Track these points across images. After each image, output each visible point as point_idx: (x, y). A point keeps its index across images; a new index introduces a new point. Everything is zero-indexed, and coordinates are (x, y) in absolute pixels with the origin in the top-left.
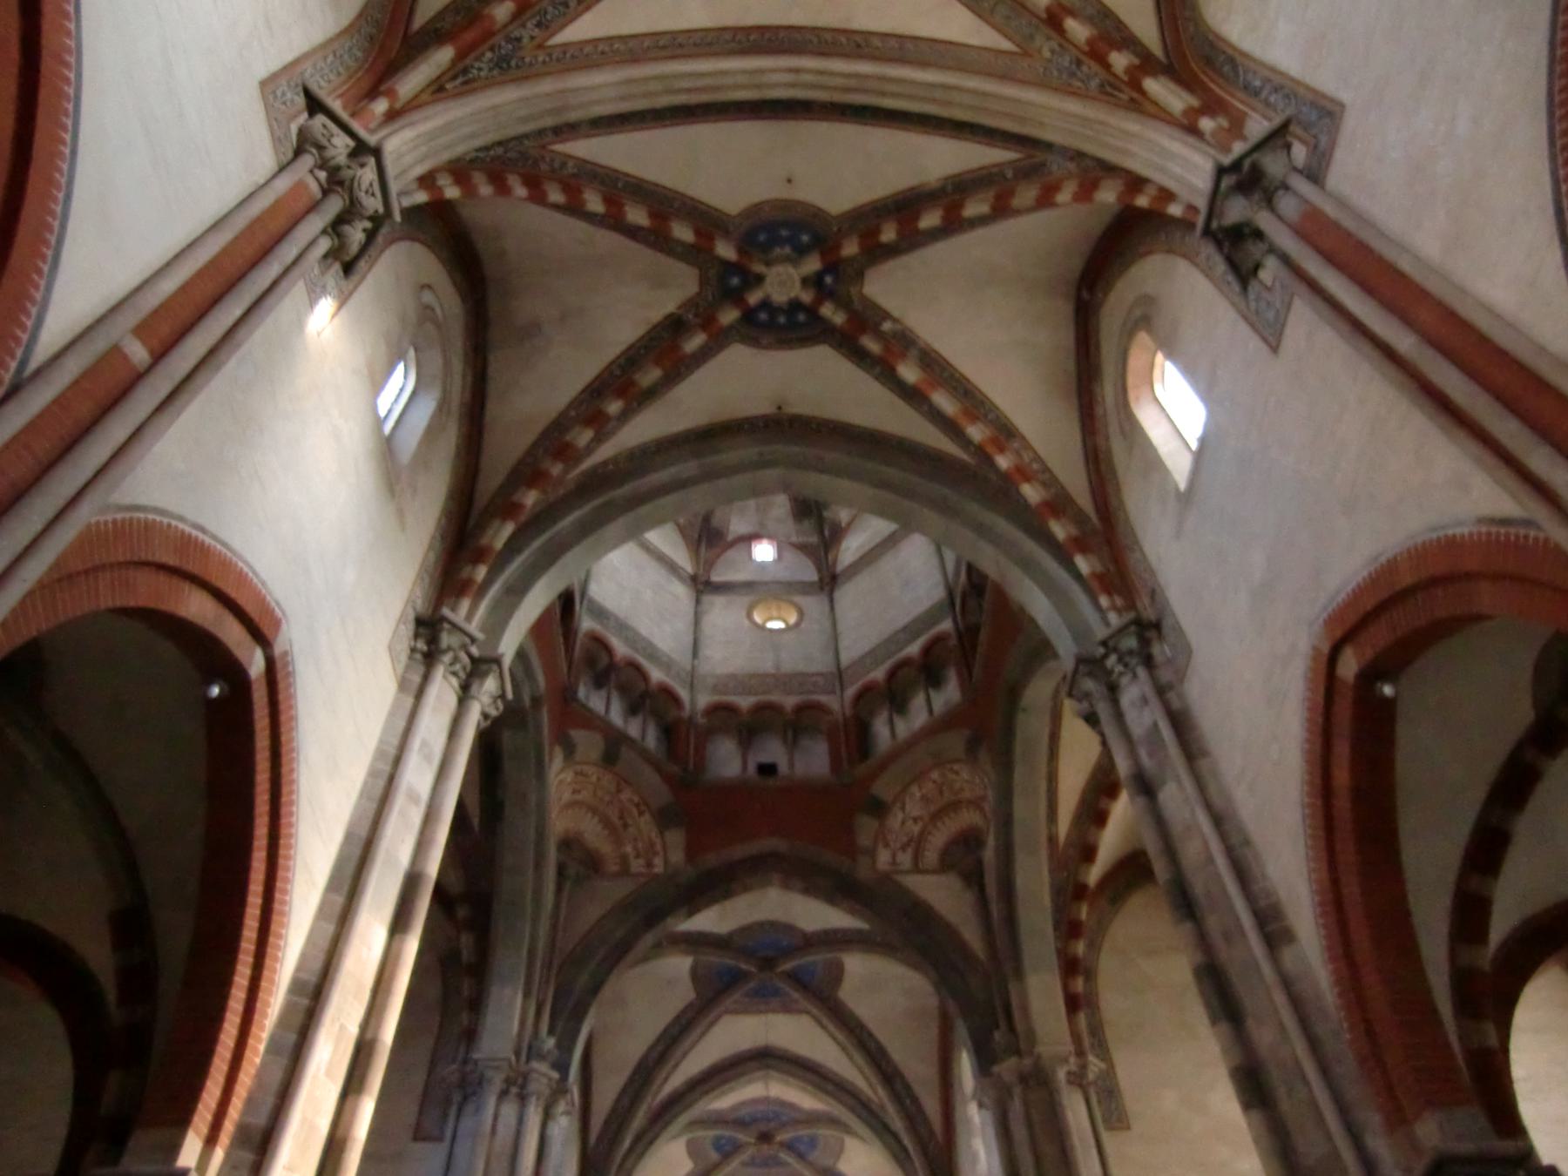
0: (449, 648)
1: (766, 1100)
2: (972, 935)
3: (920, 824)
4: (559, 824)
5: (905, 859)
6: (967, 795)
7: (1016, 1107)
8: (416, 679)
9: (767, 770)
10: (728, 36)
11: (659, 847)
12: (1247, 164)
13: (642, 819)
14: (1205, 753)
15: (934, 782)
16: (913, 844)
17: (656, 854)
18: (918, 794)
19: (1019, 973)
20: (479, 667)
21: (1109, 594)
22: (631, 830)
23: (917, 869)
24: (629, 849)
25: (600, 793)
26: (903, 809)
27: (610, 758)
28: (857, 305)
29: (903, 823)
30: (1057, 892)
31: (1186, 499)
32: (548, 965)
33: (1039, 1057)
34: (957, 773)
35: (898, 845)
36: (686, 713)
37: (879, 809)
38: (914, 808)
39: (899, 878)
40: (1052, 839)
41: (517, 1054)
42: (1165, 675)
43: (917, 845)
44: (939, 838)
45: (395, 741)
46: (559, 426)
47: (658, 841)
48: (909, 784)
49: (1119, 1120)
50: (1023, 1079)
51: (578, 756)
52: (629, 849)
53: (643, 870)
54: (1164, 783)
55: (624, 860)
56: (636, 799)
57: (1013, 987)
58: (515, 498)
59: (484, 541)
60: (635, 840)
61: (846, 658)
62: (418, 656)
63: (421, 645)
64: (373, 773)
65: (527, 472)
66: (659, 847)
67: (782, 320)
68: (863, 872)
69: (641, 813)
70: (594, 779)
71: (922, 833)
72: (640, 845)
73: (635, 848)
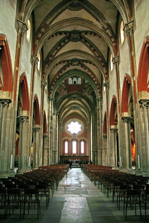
5: (87, 94)
8: (49, 102)
9: (75, 82)
23: (88, 95)
24: (61, 92)
28: (82, 64)
31: (104, 93)
32: (55, 104)
39: (87, 96)
42: (102, 102)
44: (91, 92)
46: (56, 76)
52: (61, 92)
55: (61, 93)
59: (51, 88)
65: (53, 81)
68: (83, 95)
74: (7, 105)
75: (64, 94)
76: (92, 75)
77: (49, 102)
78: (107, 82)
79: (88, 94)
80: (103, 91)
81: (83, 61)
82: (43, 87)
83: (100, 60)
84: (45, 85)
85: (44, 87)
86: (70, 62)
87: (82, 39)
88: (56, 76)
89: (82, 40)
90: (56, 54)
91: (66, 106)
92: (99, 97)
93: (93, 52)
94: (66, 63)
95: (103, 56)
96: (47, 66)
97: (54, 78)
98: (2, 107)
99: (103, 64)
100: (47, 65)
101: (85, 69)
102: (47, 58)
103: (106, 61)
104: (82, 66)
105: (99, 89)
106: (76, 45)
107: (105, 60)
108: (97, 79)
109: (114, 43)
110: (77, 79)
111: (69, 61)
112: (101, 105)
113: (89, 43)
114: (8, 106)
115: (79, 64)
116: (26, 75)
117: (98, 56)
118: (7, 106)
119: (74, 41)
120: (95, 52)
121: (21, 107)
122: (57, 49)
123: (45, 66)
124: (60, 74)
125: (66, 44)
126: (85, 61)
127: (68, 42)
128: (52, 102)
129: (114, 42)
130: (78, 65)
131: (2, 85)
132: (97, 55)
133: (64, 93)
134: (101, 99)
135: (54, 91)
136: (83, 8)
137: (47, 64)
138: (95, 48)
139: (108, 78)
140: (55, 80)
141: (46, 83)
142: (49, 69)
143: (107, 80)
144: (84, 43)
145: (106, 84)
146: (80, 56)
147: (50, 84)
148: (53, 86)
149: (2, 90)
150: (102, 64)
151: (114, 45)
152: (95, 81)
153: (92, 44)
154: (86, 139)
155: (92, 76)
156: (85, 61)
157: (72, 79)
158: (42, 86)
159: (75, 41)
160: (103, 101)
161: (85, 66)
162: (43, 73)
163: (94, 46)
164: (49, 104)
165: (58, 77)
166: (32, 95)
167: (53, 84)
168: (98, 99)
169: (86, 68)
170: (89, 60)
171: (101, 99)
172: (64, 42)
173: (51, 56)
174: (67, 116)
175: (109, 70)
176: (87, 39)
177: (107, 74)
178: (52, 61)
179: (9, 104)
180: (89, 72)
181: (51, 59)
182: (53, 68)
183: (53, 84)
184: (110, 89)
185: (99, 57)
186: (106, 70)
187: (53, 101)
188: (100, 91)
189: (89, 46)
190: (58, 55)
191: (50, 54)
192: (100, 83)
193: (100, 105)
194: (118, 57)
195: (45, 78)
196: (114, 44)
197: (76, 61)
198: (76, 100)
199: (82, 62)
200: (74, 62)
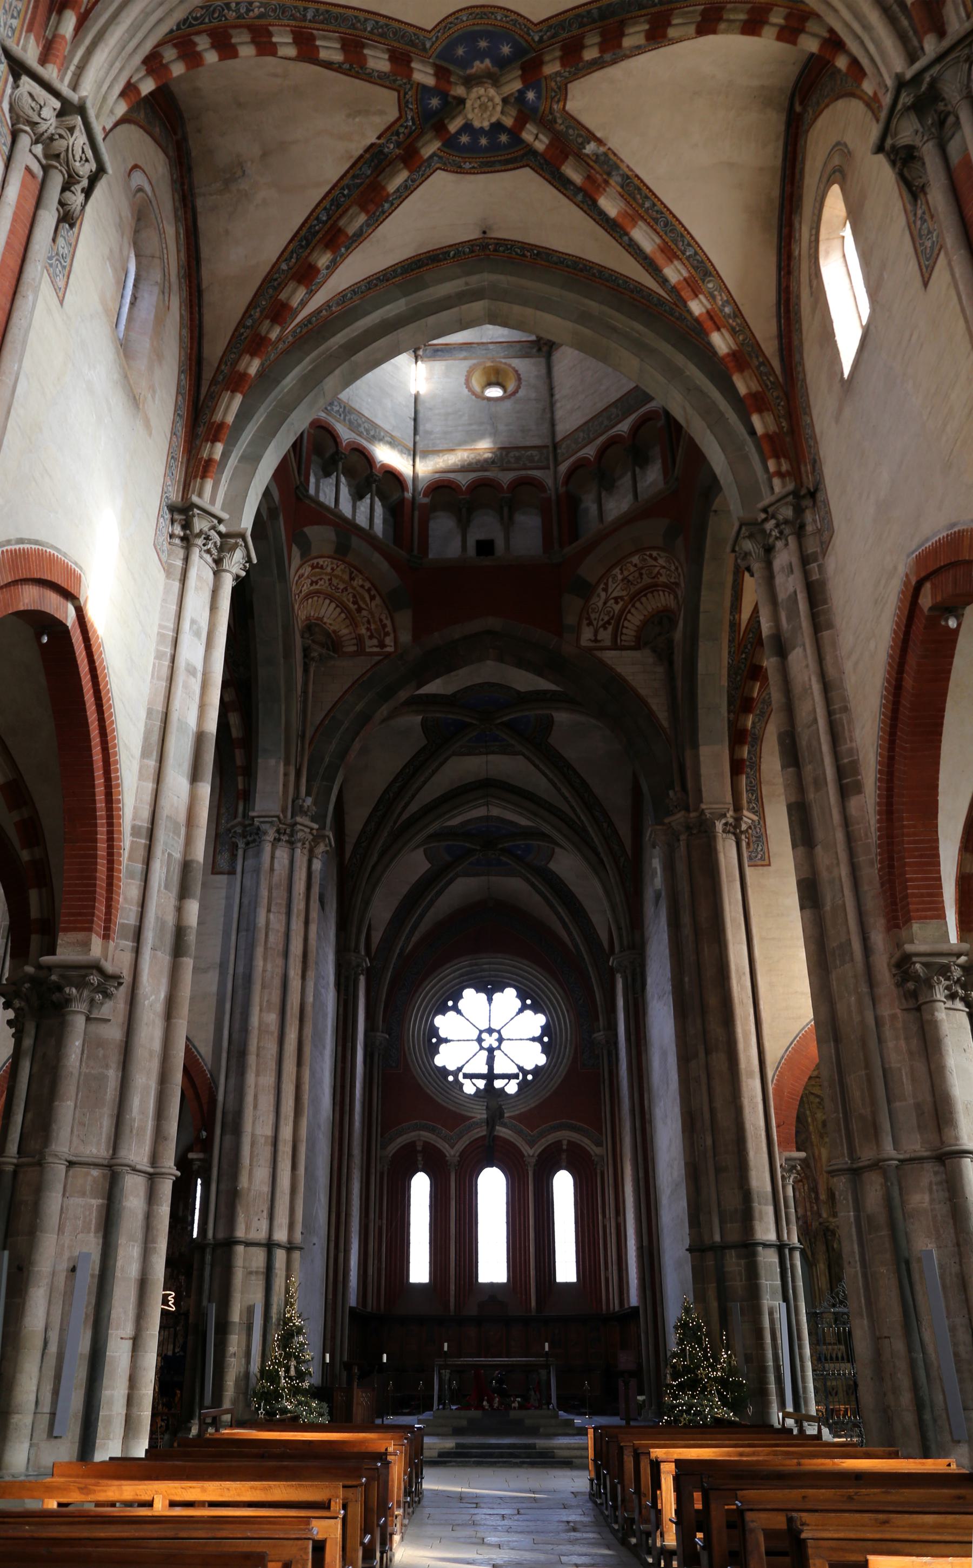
1: (487, 818)
2: (659, 706)
3: (621, 603)
4: (303, 612)
5: (605, 636)
6: (663, 579)
8: (179, 563)
9: (485, 547)
11: (389, 628)
13: (373, 604)
14: (830, 625)
15: (635, 565)
16: (613, 622)
17: (387, 634)
18: (620, 577)
20: (227, 542)
21: (777, 457)
22: (364, 613)
23: (615, 646)
25: (335, 582)
26: (605, 590)
27: (341, 551)
29: (605, 603)
30: (733, 671)
34: (655, 559)
35: (601, 623)
36: (408, 495)
37: (585, 590)
38: (617, 590)
39: (598, 653)
40: (734, 625)
41: (284, 810)
42: (812, 547)
43: (617, 622)
44: (635, 619)
45: (171, 625)
47: (388, 623)
49: (762, 859)
51: (314, 553)
54: (794, 648)
55: (360, 640)
56: (367, 585)
58: (241, 367)
59: (218, 417)
60: (369, 622)
61: (559, 437)
62: (177, 541)
63: (178, 530)
64: (159, 656)
66: (389, 628)
67: (483, 141)
69: (372, 598)
70: (329, 570)
71: (622, 611)
72: (373, 627)
73: (368, 629)
76: (670, 254)
77: (186, 560)
79: (608, 643)
84: (60, 145)
88: (280, 288)
97: (252, 305)
108: (731, 300)
110: (508, 524)
112: (806, 574)
133: (389, 641)
134: (799, 511)
136: (535, 25)
140: (267, 322)
147: (214, 382)
152: (708, 324)
154: (599, 1144)
157: (464, 525)
161: (590, 148)
164: (176, 585)
167: (244, 376)
171: (799, 511)
174: (424, 927)
183: (241, 367)
188: (773, 428)
192: (770, 348)
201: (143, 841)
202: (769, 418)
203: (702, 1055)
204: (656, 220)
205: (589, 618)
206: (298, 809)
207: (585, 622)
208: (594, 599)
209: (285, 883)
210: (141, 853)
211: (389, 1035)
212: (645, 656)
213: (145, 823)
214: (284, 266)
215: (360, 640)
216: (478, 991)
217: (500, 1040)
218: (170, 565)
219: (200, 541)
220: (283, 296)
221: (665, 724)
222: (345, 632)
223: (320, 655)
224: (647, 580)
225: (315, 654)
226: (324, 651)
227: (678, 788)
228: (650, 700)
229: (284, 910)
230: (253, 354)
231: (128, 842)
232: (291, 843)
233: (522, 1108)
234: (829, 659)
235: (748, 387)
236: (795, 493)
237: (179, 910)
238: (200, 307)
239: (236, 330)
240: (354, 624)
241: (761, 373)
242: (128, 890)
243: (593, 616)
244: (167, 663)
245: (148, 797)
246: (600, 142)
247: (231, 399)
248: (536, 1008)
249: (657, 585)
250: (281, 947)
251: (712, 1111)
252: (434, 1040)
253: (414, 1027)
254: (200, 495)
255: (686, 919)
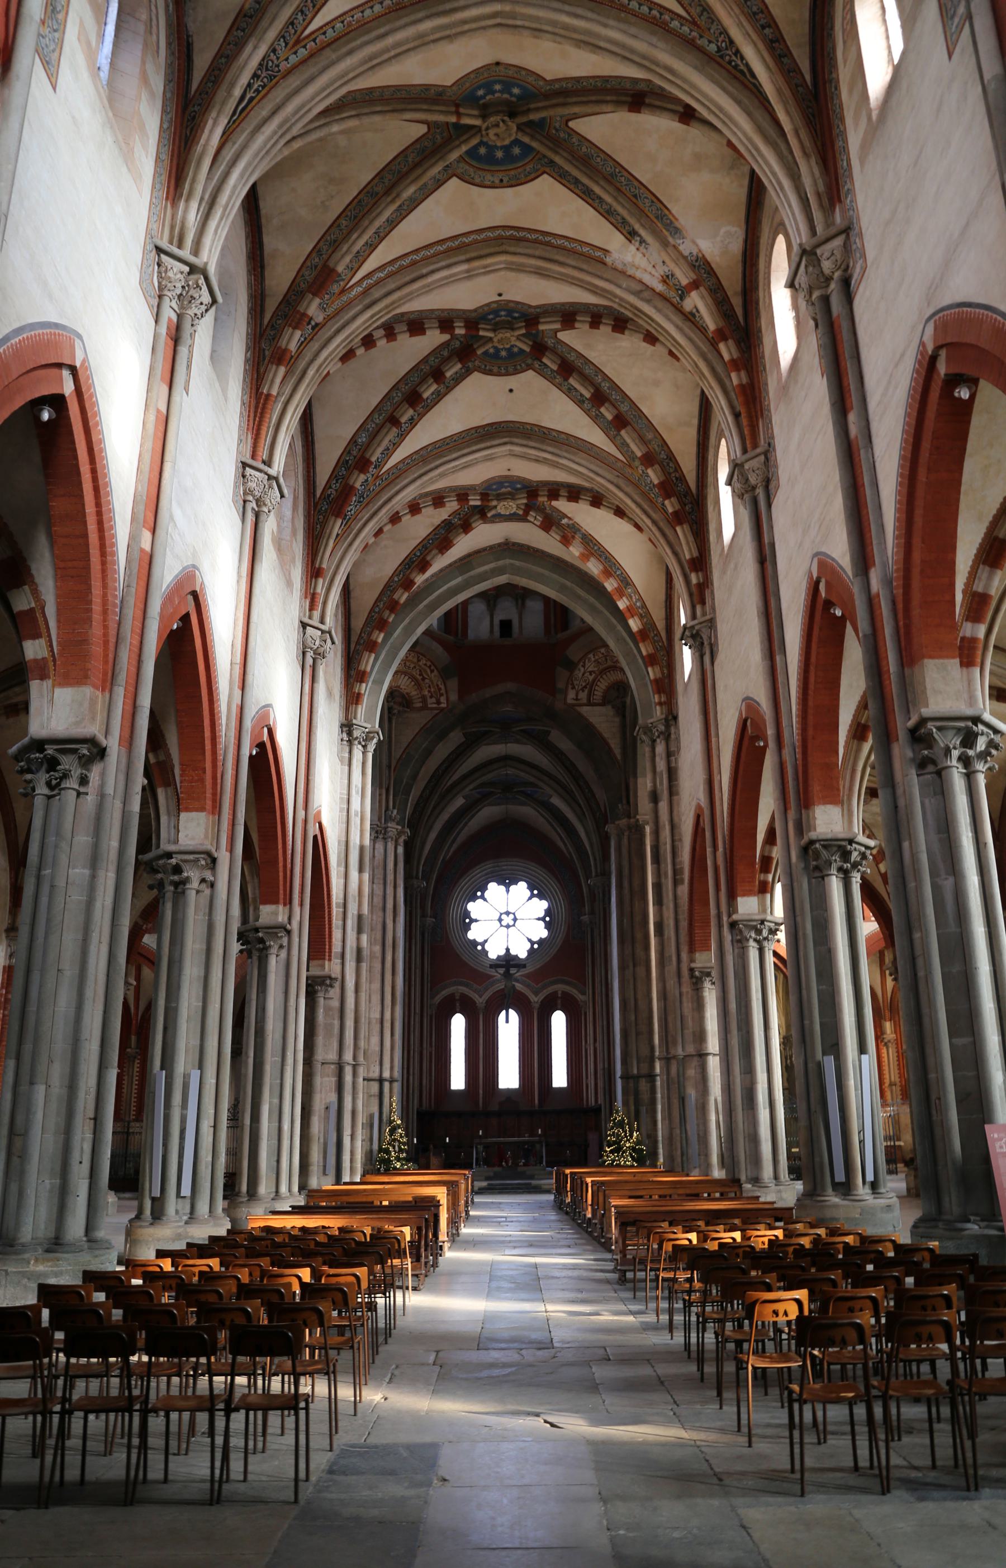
0: (357, 738)
2: (615, 745)
5: (583, 696)
7: (625, 841)
8: (347, 755)
9: (506, 626)
10: (473, 431)
11: (443, 691)
12: (697, 628)
14: (678, 794)
17: (442, 695)
19: (635, 777)
20: (368, 738)
22: (427, 681)
23: (589, 704)
24: (426, 693)
25: (408, 664)
26: (584, 666)
28: (548, 511)
31: (686, 685)
32: (389, 767)
33: (638, 820)
37: (571, 666)
38: (591, 666)
39: (578, 708)
41: (380, 820)
43: (591, 687)
44: (603, 685)
45: (345, 792)
46: (389, 588)
47: (442, 687)
48: (589, 652)
50: (629, 828)
52: (426, 693)
53: (435, 706)
55: (424, 699)
56: (429, 663)
57: (631, 780)
58: (374, 637)
59: (362, 667)
63: (345, 737)
64: (341, 811)
69: (432, 671)
71: (594, 680)
74: (76, 772)
75: (443, 705)
76: (607, 573)
77: (350, 752)
78: (704, 614)
79: (585, 701)
80: (678, 677)
81: (554, 490)
82: (309, 661)
83: (656, 482)
84: (321, 650)
85: (314, 660)
86: (475, 501)
87: (543, 355)
88: (394, 591)
89: (545, 360)
90: (388, 453)
91: (456, 777)
92: (659, 712)
93: (613, 432)
94: (452, 505)
95: (671, 457)
96: (337, 526)
97: (378, 600)
98: (46, 791)
99: (670, 506)
100: (339, 522)
101: (566, 541)
102: (334, 475)
103: (693, 486)
104: (550, 522)
105: (651, 660)
106: (511, 391)
107: (682, 478)
108: (641, 599)
109: (738, 370)
110: (521, 607)
111: (467, 495)
112: (669, 762)
113: (585, 379)
114: (84, 781)
115: (528, 508)
116: (202, 583)
117: (639, 454)
118: (76, 787)
119: (495, 369)
120: (623, 433)
121: (170, 790)
122: (393, 421)
123: (323, 525)
124: (420, 579)
125: (449, 389)
126: (563, 492)
127: (459, 379)
128: (364, 753)
129: (735, 365)
130: (523, 518)
131: (51, 646)
132: (633, 447)
133: (443, 699)
134: (668, 726)
135: (383, 683)
136: (544, 172)
137: (337, 516)
138: (624, 408)
139: (707, 593)
140: (387, 612)
141: (330, 633)
142: (350, 544)
143: (703, 603)
144: (559, 379)
145: (693, 627)
146: (537, 461)
147: (358, 643)
148: (371, 652)
149: (50, 682)
150: (667, 502)
151: (735, 381)
152: (627, 615)
153: (605, 386)
155: (610, 585)
156: (563, 492)
158: (304, 653)
159: (503, 371)
160: (678, 739)
161: (565, 521)
162: (313, 572)
163: (614, 396)
164: (347, 768)
165: (406, 596)
166: (242, 708)
167: (375, 643)
168: (648, 730)
169: (569, 533)
170: (586, 484)
171: (668, 726)
172: (438, 375)
173: (363, 464)
175: (712, 537)
176: (572, 357)
177: (700, 563)
178: (366, 499)
179: (88, 770)
180: (592, 559)
181: (358, 485)
182: (372, 540)
183: (374, 637)
184: (720, 658)
185: (649, 460)
186: (691, 539)
187: (372, 747)
188: (659, 675)
189: (588, 395)
190: (403, 461)
191: (355, 453)
192: (661, 625)
193: (661, 765)
194: (766, 453)
195: (325, 603)
196: (733, 375)
197: (512, 496)
198: (517, 742)
199: (546, 499)
200: (500, 497)
201: (341, 910)
202: (657, 669)
203: (631, 967)
204: (600, 556)
205: (573, 684)
206: (388, 818)
207: (570, 687)
208: (577, 672)
209: (382, 863)
210: (341, 916)
211: (435, 918)
212: (608, 710)
213: (342, 901)
214: (396, 579)
215: (424, 699)
216: (499, 884)
217: (515, 920)
218: (343, 757)
219: (356, 742)
220: (396, 597)
221: (619, 757)
222: (414, 693)
223: (399, 712)
224: (609, 663)
225: (396, 711)
226: (401, 709)
227: (624, 802)
228: (610, 741)
229: (382, 882)
230: (381, 631)
231: (336, 911)
232: (384, 838)
233: (529, 969)
234: (675, 813)
235: (647, 651)
236: (666, 720)
237: (358, 939)
238: (349, 598)
239: (370, 613)
240: (418, 685)
241: (655, 641)
242: (337, 935)
243: (575, 682)
244: (345, 814)
245: (342, 887)
246: (570, 518)
247: (369, 657)
248: (541, 896)
249: (616, 667)
250: (381, 905)
251: (636, 1000)
252: (467, 921)
253: (453, 913)
254: (355, 718)
255: (626, 884)
